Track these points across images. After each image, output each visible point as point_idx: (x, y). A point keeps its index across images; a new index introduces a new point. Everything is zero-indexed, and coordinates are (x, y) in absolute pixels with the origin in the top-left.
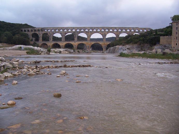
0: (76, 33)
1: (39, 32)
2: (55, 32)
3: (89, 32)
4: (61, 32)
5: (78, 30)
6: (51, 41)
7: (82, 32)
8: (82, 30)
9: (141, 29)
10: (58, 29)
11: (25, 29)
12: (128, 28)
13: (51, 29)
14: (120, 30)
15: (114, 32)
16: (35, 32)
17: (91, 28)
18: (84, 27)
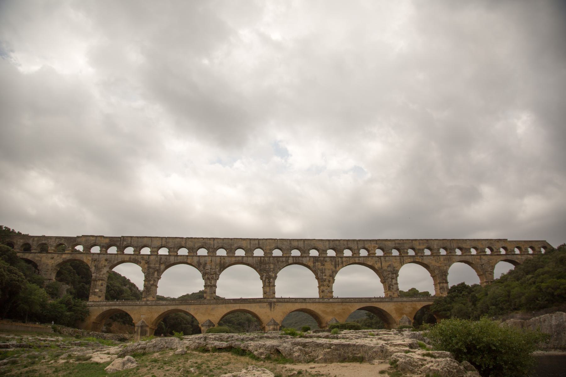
0: (272, 266)
2: (172, 259)
3: (328, 259)
4: (202, 260)
5: (277, 253)
6: (150, 298)
8: (296, 253)
9: (519, 245)
10: (190, 244)
11: (30, 242)
12: (474, 244)
13: (157, 243)
14: (443, 252)
15: (425, 262)
17: (332, 245)
18: (304, 240)
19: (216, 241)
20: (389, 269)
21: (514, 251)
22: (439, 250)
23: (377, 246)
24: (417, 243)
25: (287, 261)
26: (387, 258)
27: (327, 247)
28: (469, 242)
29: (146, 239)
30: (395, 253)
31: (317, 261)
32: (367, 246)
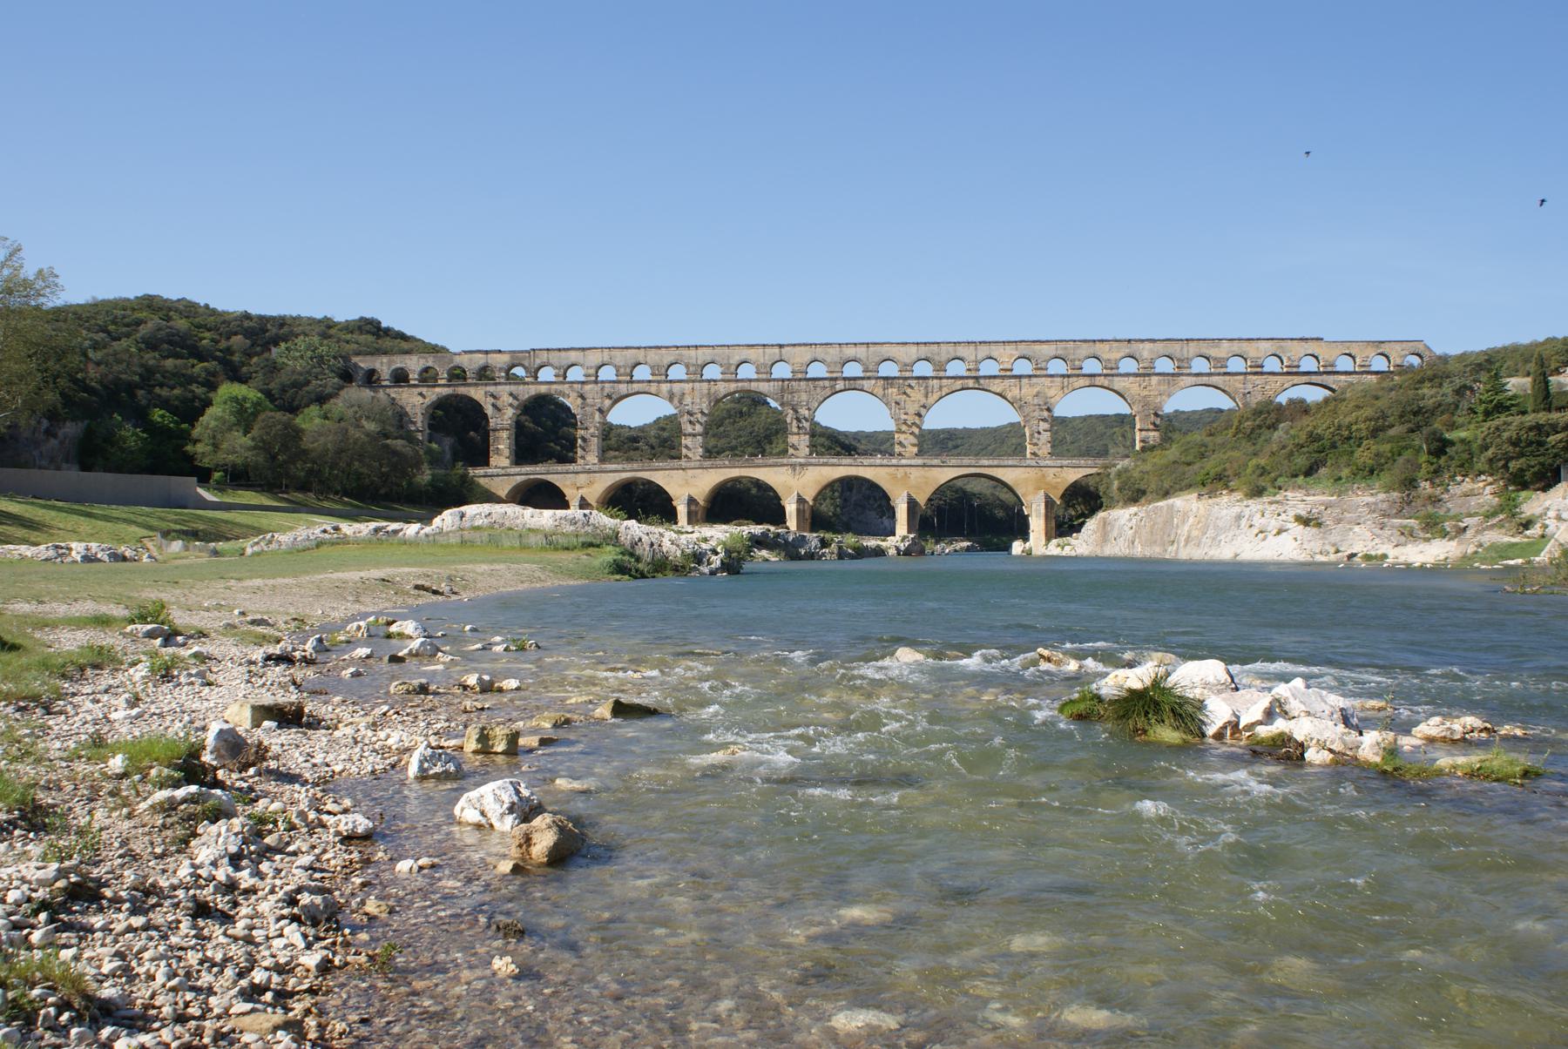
0: (804, 397)
1: (491, 389)
5: (817, 370)
7: (852, 384)
8: (853, 370)
12: (1236, 347)
13: (594, 358)
15: (1119, 383)
16: (462, 390)
17: (924, 351)
19: (700, 351)
20: (1036, 401)
21: (1332, 365)
22: (1152, 361)
23: (1017, 354)
24: (1106, 346)
25: (832, 387)
26: (1034, 380)
27: (914, 357)
28: (1225, 344)
29: (573, 354)
30: (1057, 367)
31: (892, 386)
32: (994, 354)
